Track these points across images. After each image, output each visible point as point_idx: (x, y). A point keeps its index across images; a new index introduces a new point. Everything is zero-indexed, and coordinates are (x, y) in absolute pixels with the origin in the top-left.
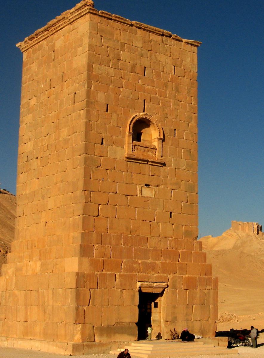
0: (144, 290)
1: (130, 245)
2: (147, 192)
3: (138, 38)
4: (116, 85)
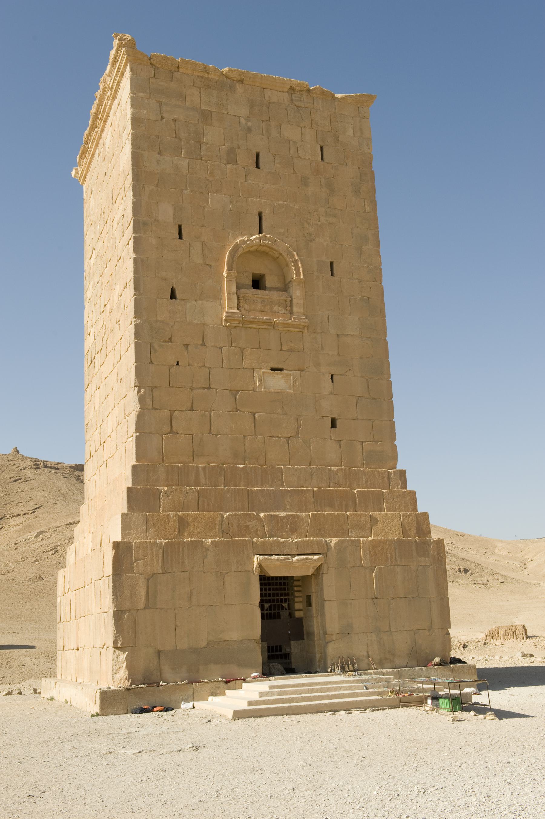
0: (272, 573)
2: (277, 383)
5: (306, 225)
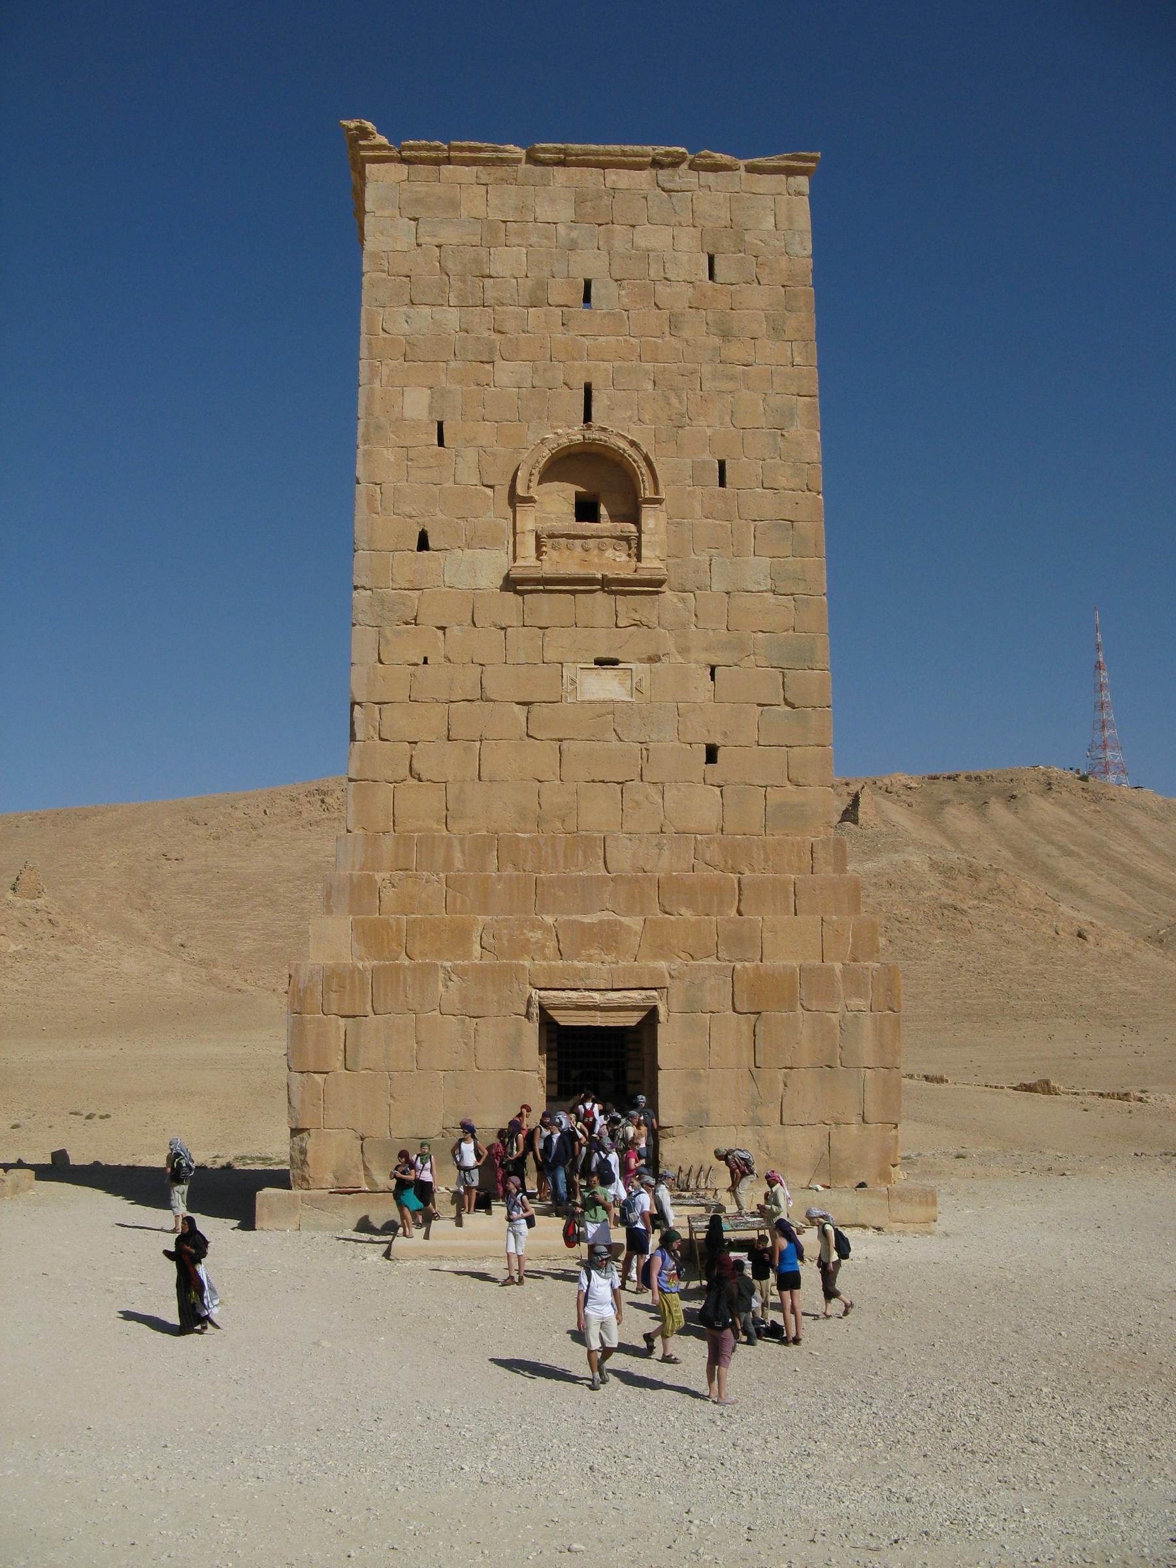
0: (565, 1019)
1: (529, 867)
2: (605, 687)
3: (555, 196)
4: (471, 357)
5: (674, 401)
